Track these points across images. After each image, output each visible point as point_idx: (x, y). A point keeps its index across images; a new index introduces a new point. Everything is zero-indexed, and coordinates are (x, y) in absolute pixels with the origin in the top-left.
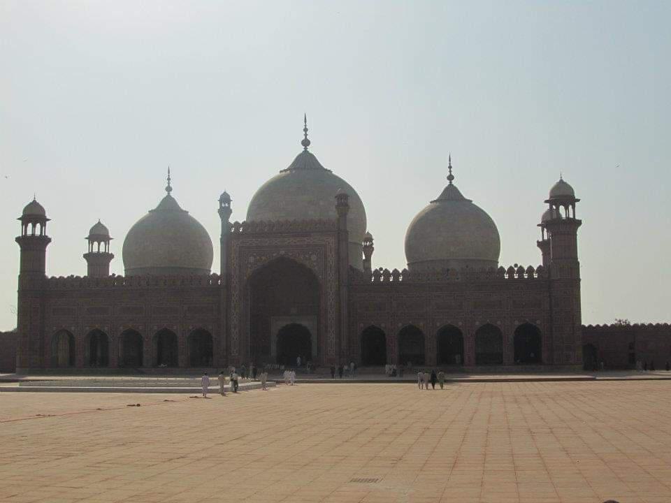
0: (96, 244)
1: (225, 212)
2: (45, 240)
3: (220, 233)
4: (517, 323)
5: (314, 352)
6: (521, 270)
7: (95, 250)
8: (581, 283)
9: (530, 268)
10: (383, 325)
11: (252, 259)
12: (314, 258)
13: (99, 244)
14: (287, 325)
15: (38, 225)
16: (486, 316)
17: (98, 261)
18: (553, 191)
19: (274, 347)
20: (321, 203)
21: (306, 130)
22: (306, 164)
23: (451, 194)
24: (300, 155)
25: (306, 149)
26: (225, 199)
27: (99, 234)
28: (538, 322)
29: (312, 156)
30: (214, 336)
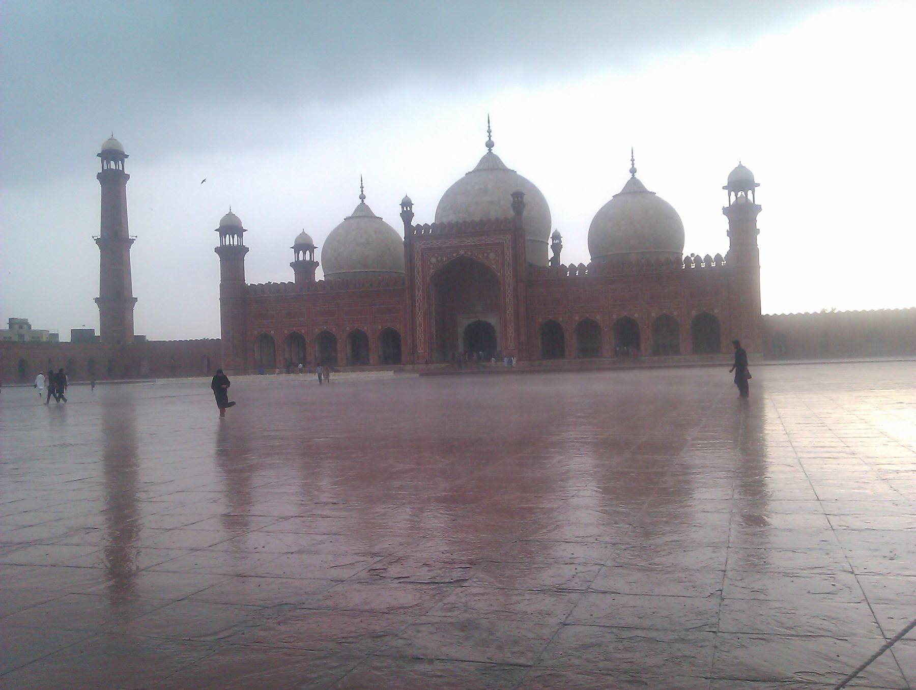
1: (407, 216)
2: (243, 250)
4: (694, 312)
6: (698, 259)
7: (301, 259)
9: (718, 256)
11: (433, 260)
13: (304, 253)
17: (304, 269)
19: (461, 344)
20: (502, 203)
22: (491, 164)
23: (634, 188)
24: (484, 158)
25: (490, 150)
26: (407, 204)
27: (303, 245)
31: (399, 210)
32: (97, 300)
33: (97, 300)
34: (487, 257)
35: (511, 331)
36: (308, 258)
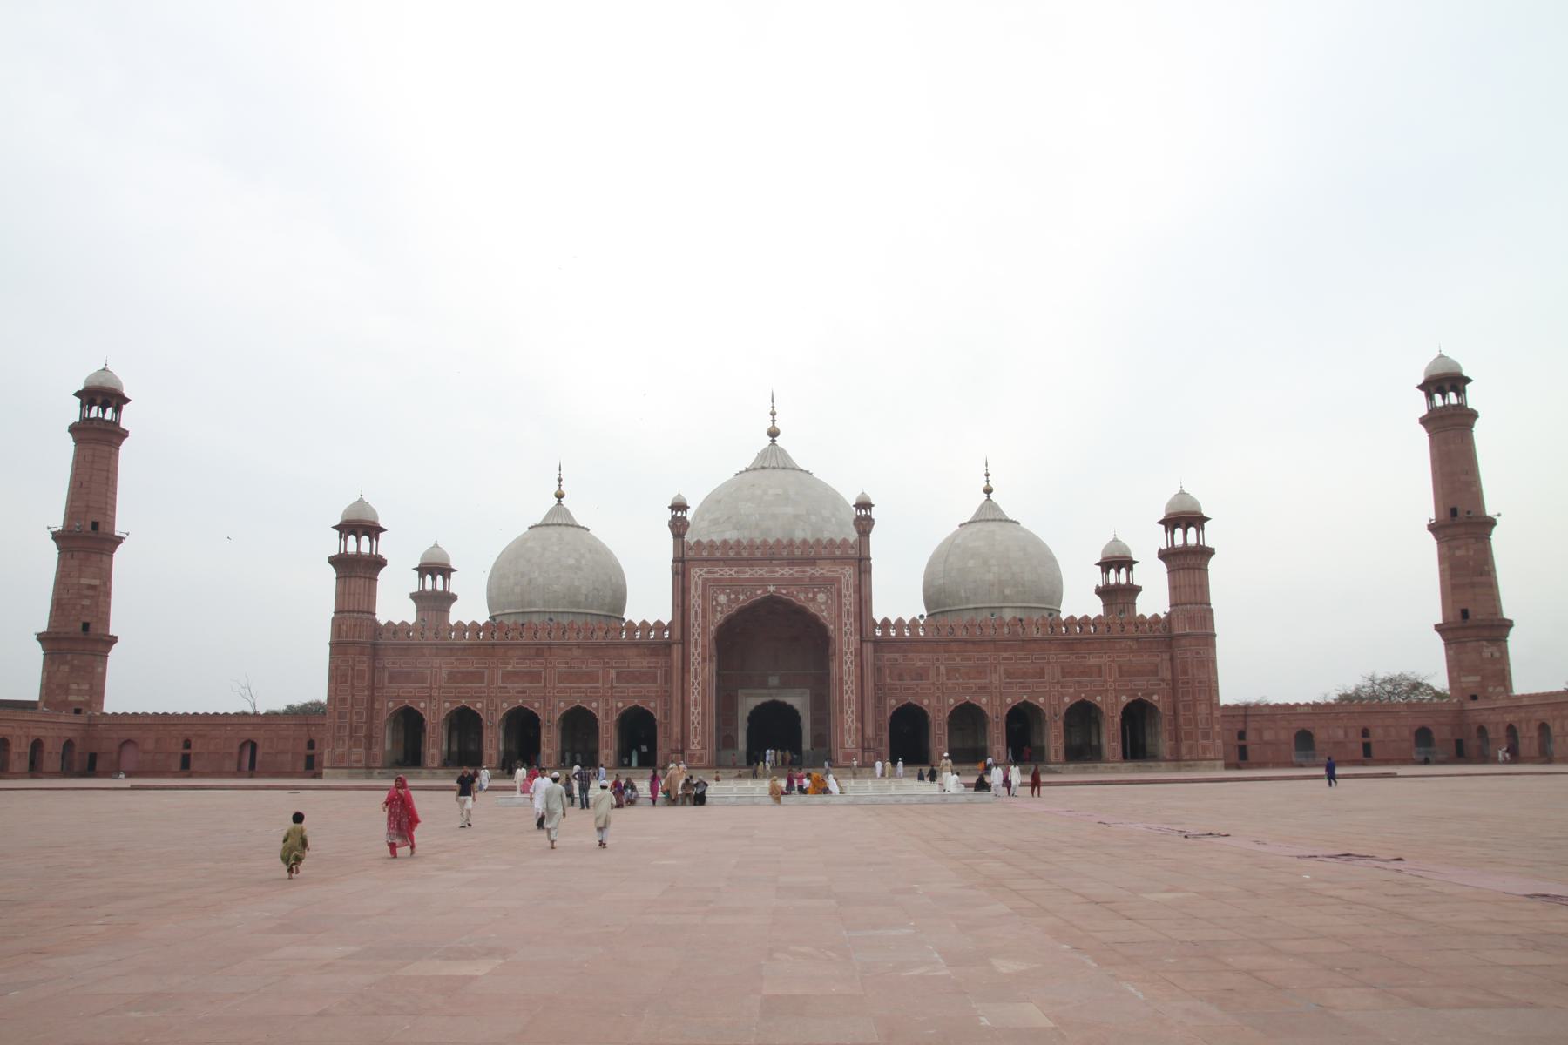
0: (429, 577)
3: (670, 556)
4: (1125, 699)
5: (806, 745)
7: (429, 586)
8: (1217, 639)
10: (926, 702)
11: (722, 599)
12: (821, 597)
13: (434, 579)
14: (764, 704)
15: (365, 540)
16: (1087, 692)
18: (1171, 504)
20: (813, 518)
21: (773, 414)
23: (989, 514)
28: (1155, 697)
29: (783, 453)
30: (657, 717)
31: (668, 515)
32: (41, 638)
33: (41, 638)
34: (814, 599)
35: (850, 719)
36: (440, 587)
